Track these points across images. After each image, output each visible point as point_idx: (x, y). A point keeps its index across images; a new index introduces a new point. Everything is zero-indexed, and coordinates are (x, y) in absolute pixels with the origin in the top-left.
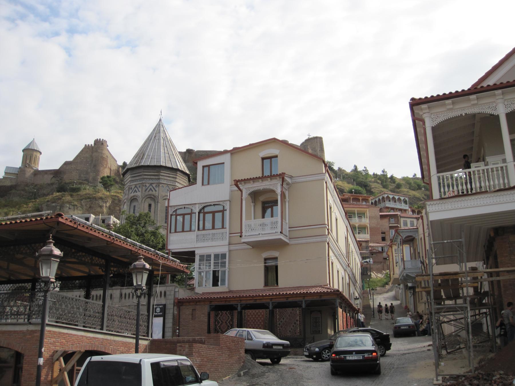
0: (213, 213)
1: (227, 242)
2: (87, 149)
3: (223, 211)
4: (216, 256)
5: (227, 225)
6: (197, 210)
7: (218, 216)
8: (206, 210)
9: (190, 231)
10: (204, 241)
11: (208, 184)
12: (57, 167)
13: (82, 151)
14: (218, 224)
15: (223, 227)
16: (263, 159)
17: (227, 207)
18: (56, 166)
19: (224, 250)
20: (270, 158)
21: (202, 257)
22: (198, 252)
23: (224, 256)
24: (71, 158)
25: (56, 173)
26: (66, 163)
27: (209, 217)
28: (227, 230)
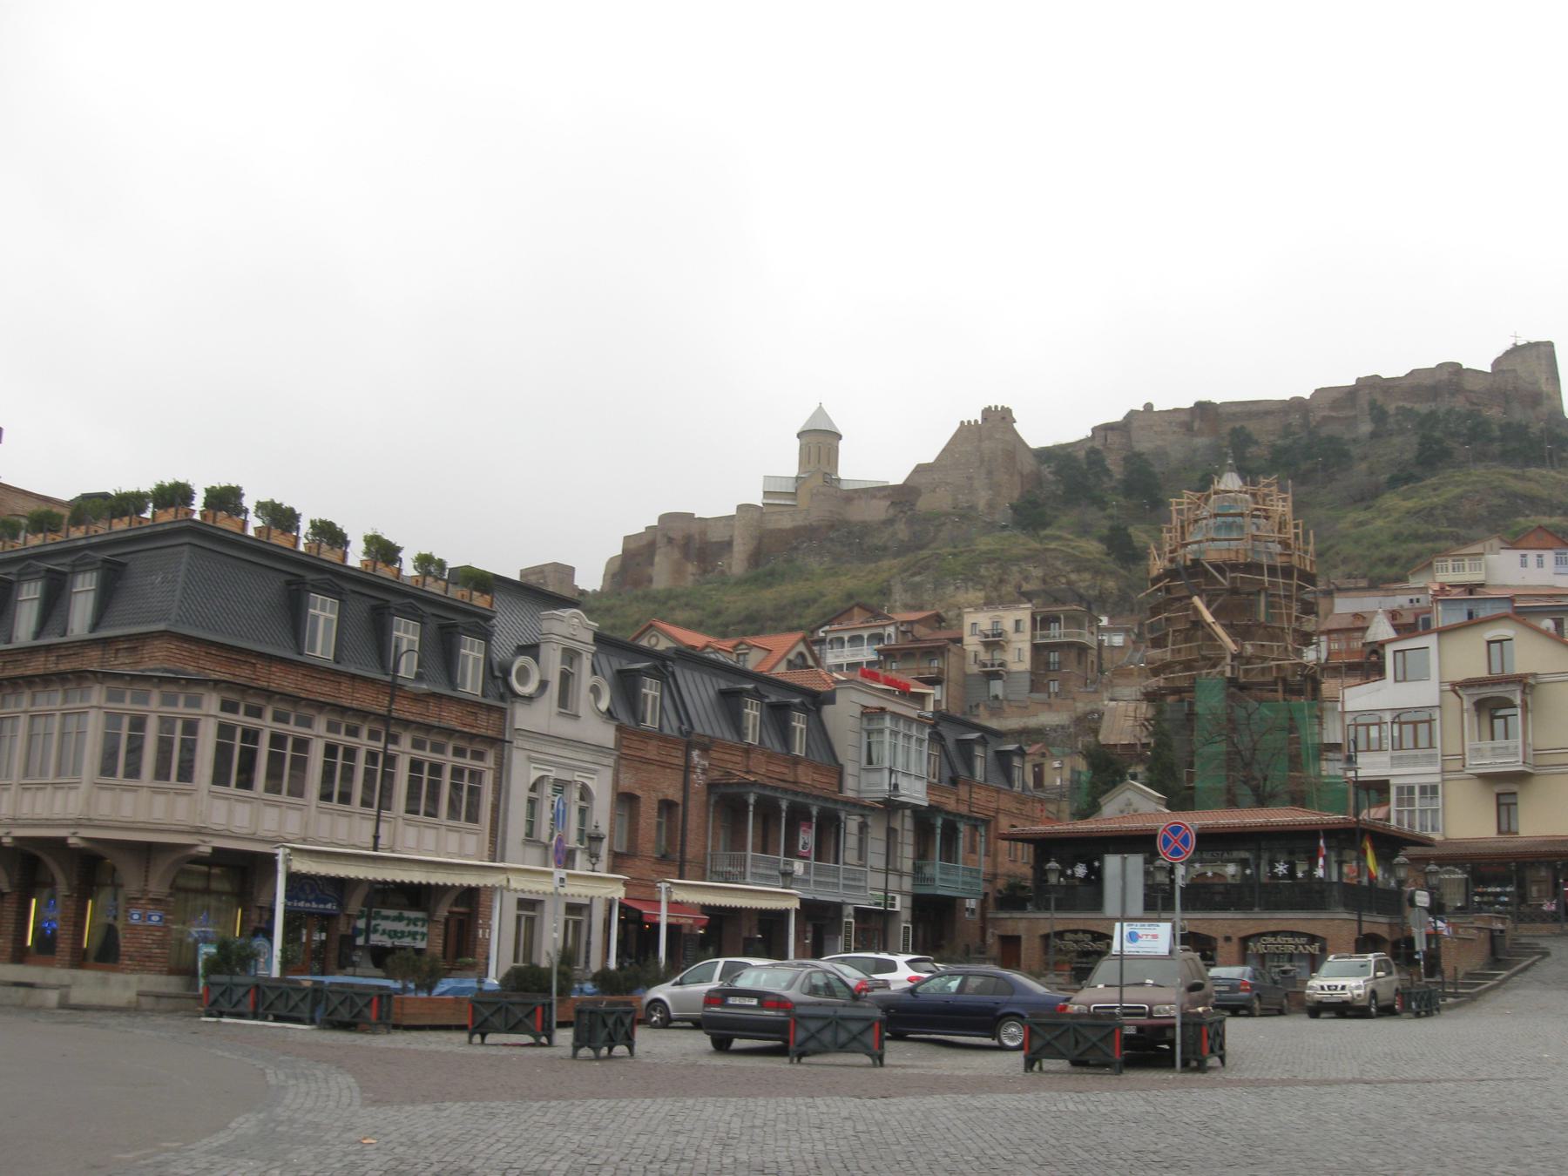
0: (1415, 723)
1: (1437, 769)
2: (965, 430)
3: (1430, 721)
4: (1423, 789)
5: (1438, 743)
6: (1388, 717)
7: (1423, 728)
8: (1403, 718)
9: (1380, 750)
10: (1400, 765)
11: (1405, 680)
12: (897, 477)
13: (955, 436)
14: (1423, 742)
15: (1431, 746)
16: (1489, 642)
17: (1437, 715)
18: (896, 474)
19: (1437, 779)
20: (1500, 641)
21: (1400, 789)
22: (1393, 781)
23: (1434, 789)
24: (929, 457)
25: (901, 496)
26: (920, 469)
27: (1408, 729)
28: (1438, 751)
